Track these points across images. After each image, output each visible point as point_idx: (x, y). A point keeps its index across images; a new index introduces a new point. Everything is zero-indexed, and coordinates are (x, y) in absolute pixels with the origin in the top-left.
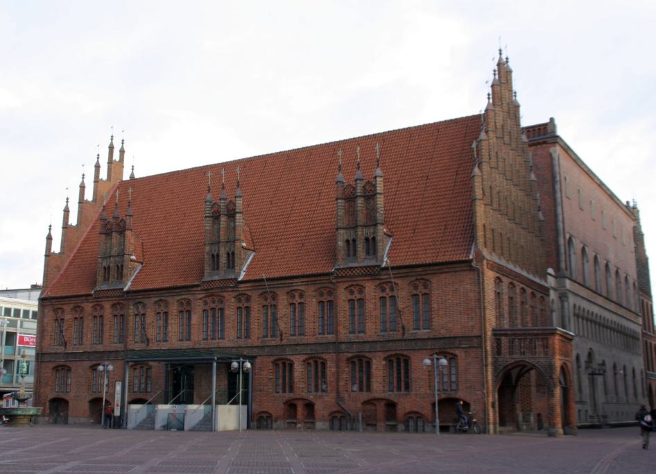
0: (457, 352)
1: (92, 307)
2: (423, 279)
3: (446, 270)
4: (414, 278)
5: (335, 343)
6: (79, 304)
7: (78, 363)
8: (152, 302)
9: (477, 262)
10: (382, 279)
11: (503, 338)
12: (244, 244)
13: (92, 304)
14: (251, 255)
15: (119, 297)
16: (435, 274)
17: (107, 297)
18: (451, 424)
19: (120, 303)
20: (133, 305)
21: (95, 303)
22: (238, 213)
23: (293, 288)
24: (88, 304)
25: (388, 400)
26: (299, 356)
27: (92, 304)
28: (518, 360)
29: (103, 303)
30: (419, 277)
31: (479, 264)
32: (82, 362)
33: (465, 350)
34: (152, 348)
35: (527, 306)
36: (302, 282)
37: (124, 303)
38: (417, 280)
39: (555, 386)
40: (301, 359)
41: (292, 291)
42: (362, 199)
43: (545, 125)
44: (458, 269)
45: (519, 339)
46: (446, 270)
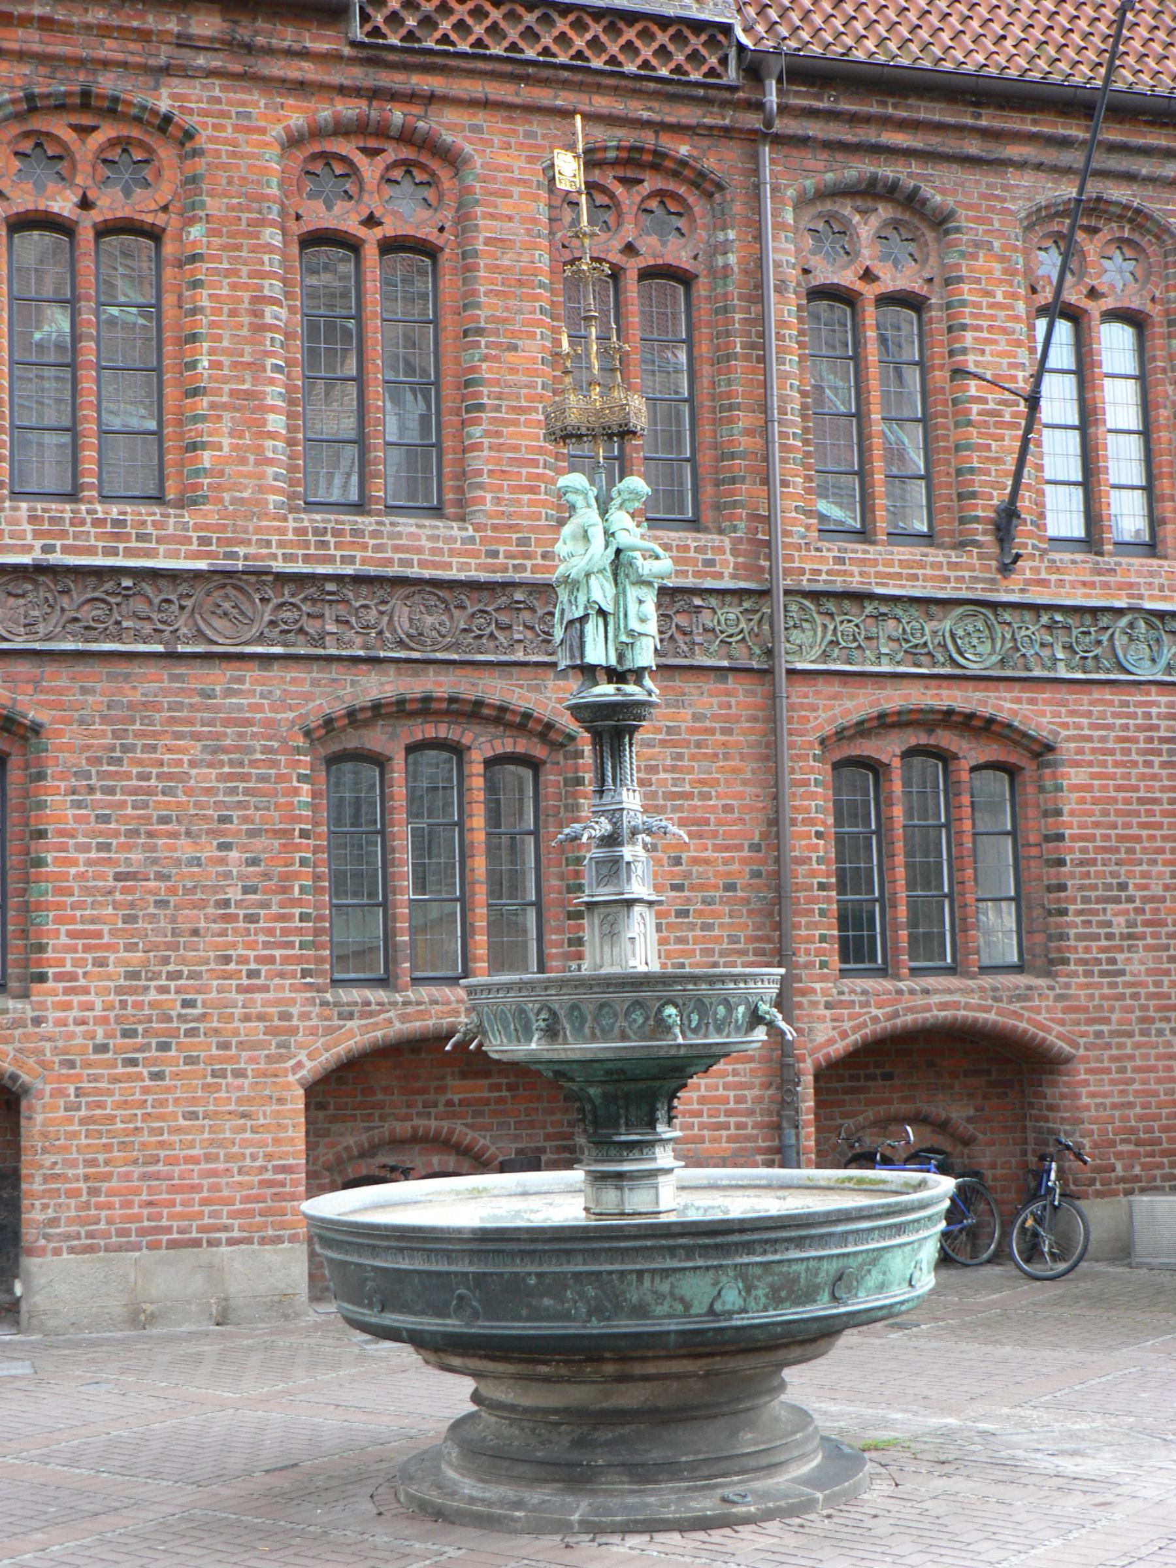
1: (293, 141)
6: (107, 83)
7: (152, 683)
8: (1019, 207)
13: (296, 115)
15: (674, 91)
17: (517, 70)
19: (658, 162)
20: (802, 202)
21: (350, 109)
24: (258, 102)
27: (296, 115)
29: (449, 126)
32: (218, 677)
34: (1037, 596)
37: (709, 163)
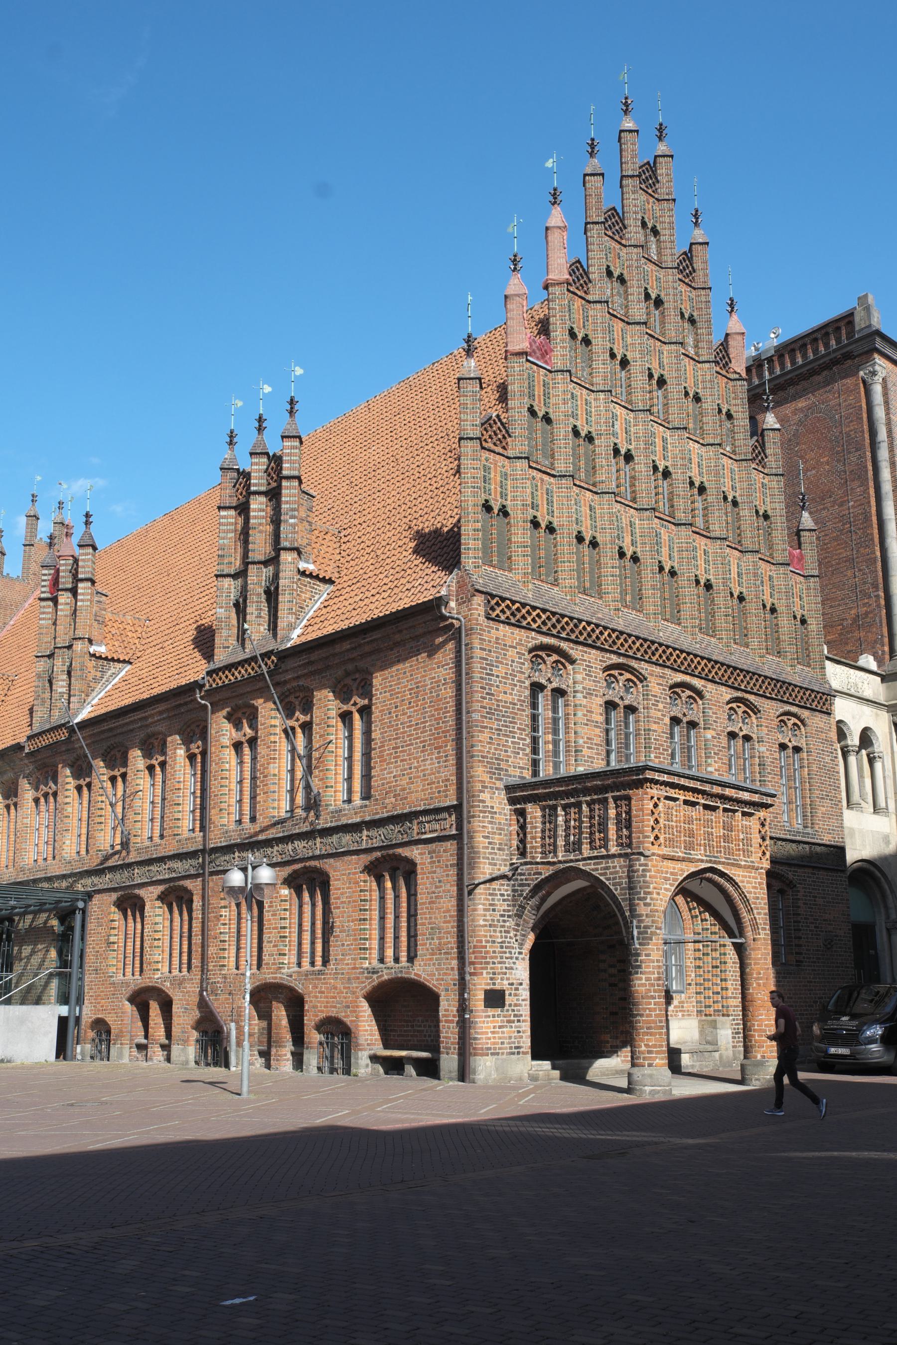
0: (414, 853)
2: (357, 670)
3: (398, 637)
4: (340, 673)
5: (203, 851)
9: (459, 604)
10: (285, 682)
11: (530, 807)
12: (101, 650)
14: (121, 670)
16: (378, 651)
18: (403, 1053)
22: (82, 580)
23: (150, 730)
25: (291, 990)
26: (151, 888)
28: (562, 866)
30: (350, 667)
31: (464, 608)
33: (433, 846)
35: (709, 734)
36: (161, 713)
38: (347, 674)
39: (645, 939)
40: (155, 895)
41: (149, 736)
42: (263, 499)
43: (848, 319)
44: (420, 631)
45: (565, 807)
46: (398, 637)
